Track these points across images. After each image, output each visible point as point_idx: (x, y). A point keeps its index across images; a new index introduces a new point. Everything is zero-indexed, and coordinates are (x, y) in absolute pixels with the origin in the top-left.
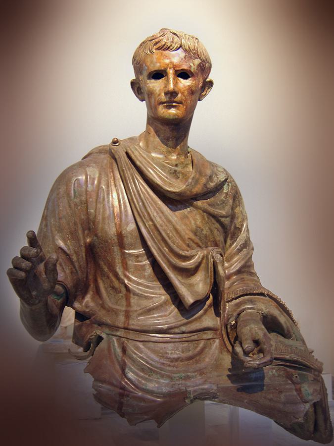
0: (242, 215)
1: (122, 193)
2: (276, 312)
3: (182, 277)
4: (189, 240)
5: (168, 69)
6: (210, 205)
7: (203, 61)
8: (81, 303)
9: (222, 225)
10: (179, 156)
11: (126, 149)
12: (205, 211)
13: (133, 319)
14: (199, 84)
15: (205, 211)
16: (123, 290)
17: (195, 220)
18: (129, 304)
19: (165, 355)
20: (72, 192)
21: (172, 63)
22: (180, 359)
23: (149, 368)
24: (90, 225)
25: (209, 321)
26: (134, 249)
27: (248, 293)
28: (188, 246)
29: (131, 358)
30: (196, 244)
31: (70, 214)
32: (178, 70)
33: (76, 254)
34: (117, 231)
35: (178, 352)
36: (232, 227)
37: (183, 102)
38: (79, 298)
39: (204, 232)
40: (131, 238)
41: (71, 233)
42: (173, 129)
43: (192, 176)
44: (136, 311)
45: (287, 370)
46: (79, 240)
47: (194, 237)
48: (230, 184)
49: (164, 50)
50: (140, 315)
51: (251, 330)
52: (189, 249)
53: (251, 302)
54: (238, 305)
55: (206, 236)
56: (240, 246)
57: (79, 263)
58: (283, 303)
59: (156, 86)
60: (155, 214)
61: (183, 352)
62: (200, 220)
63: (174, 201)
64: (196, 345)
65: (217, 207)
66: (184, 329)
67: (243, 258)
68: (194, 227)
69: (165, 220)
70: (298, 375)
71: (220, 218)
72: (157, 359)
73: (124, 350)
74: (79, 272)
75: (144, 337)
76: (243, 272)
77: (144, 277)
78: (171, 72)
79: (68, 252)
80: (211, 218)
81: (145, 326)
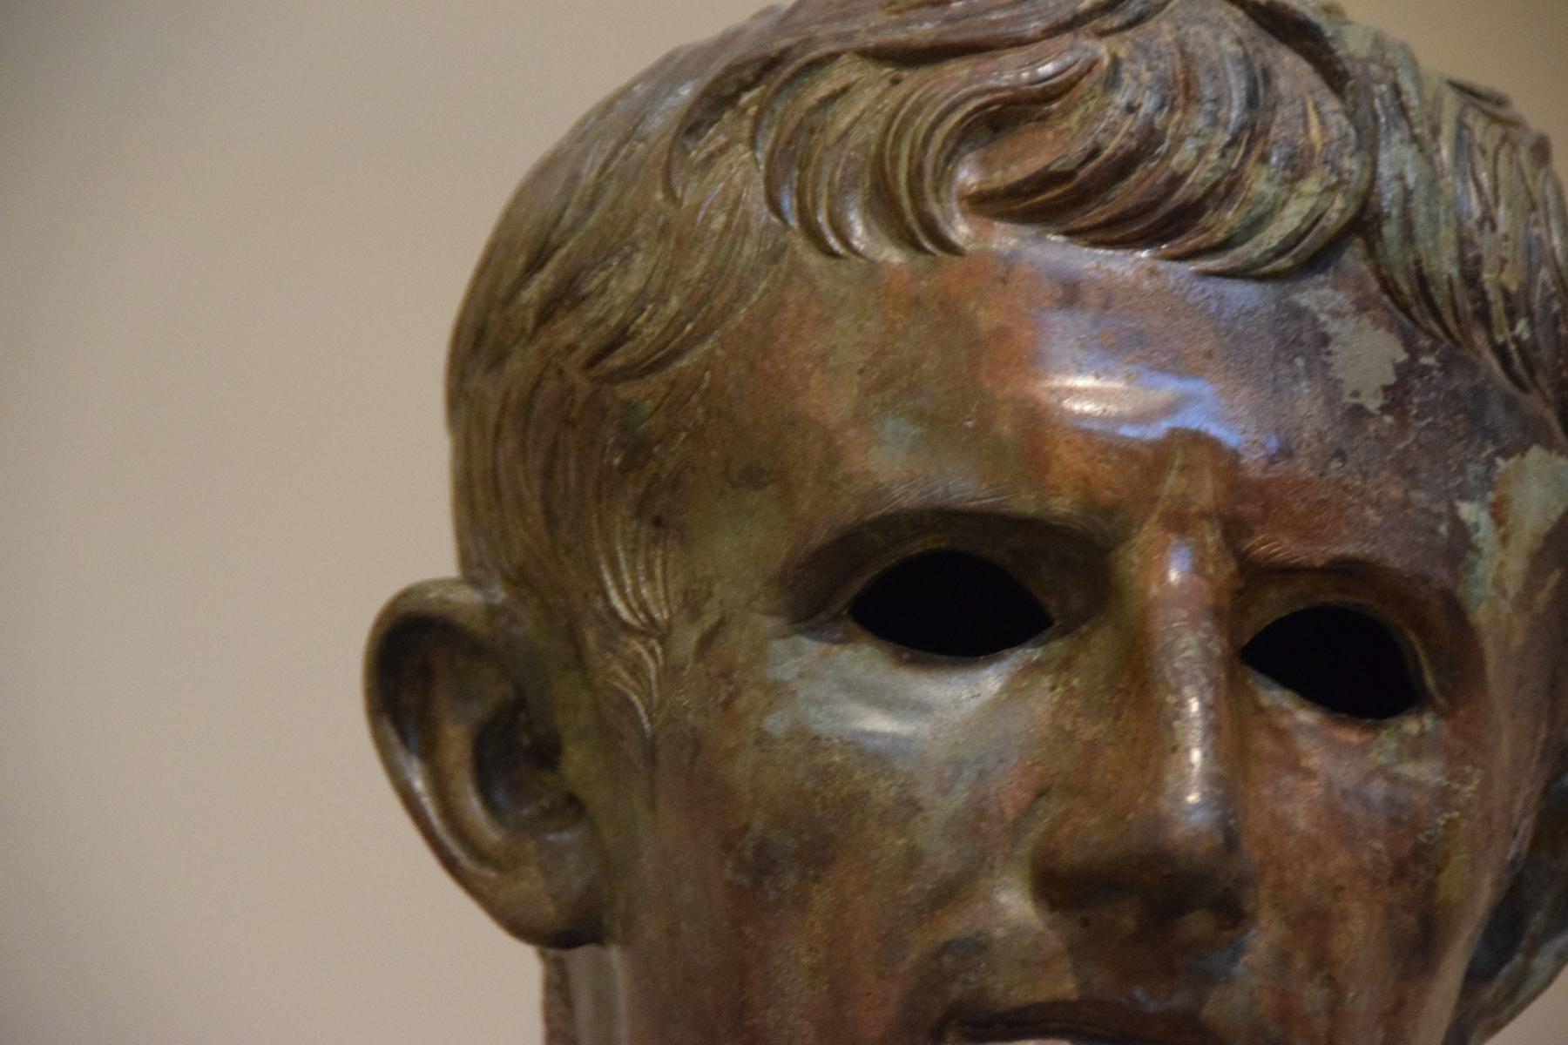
5: (1148, 533)
32: (1287, 572)
49: (1117, 233)
59: (934, 725)
78: (1173, 572)
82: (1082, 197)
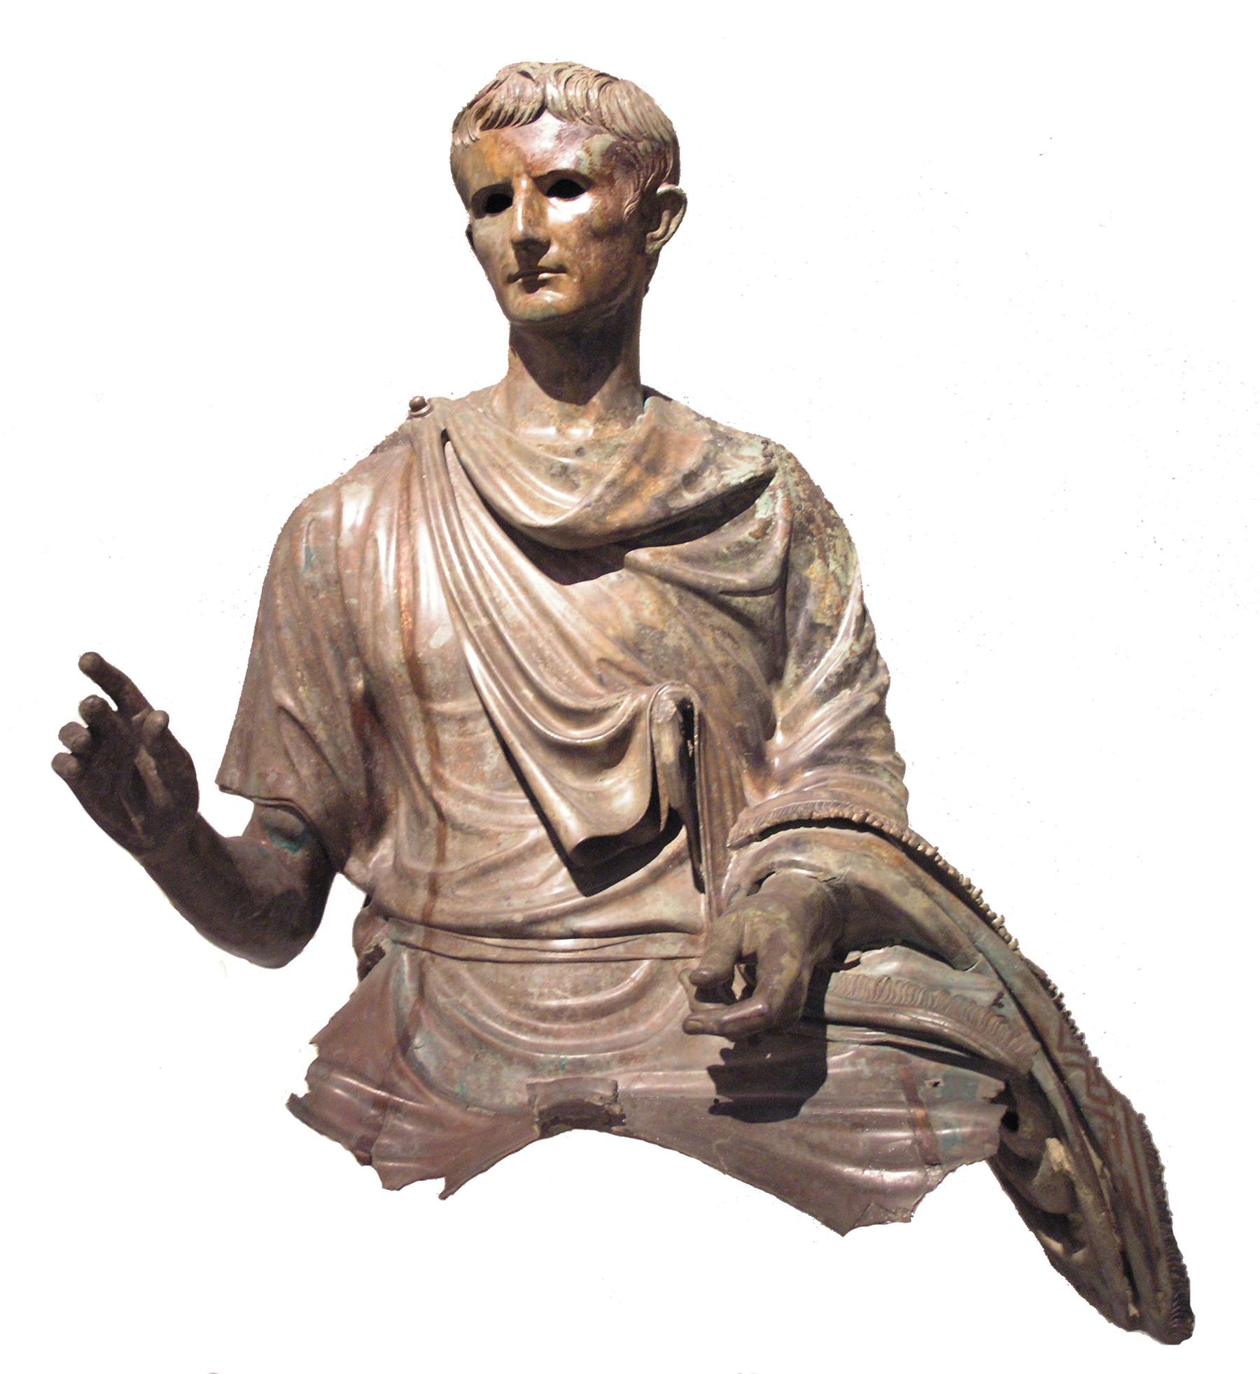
1: (444, 546)
3: (575, 771)
4: (604, 665)
6: (686, 559)
7: (626, 136)
8: (365, 862)
9: (736, 614)
10: (600, 426)
11: (445, 423)
12: (665, 578)
13: (445, 896)
14: (619, 206)
15: (665, 578)
16: (433, 815)
18: (441, 858)
19: (523, 1000)
20: (302, 555)
21: (521, 157)
22: (567, 1013)
23: (474, 1035)
24: (351, 641)
25: (666, 904)
26: (455, 697)
27: (795, 817)
28: (600, 681)
29: (434, 1006)
30: (631, 674)
31: (299, 613)
33: (326, 722)
34: (405, 650)
35: (559, 992)
36: (801, 625)
37: (568, 265)
38: (360, 846)
39: (670, 641)
40: (443, 669)
41: (309, 667)
42: (582, 346)
43: (609, 477)
44: (452, 873)
45: (906, 1061)
46: (329, 685)
47: (619, 657)
48: (780, 494)
50: (463, 882)
51: (738, 926)
52: (600, 691)
53: (796, 844)
55: (678, 653)
56: (826, 680)
57: (335, 745)
58: (929, 852)
60: (505, 595)
61: (576, 992)
62: (652, 607)
63: (567, 555)
64: (619, 974)
65: (717, 563)
67: (834, 719)
68: (632, 626)
69: (533, 612)
70: (945, 1078)
71: (727, 597)
72: (501, 1009)
74: (339, 772)
75: (470, 947)
76: (835, 761)
77: (482, 778)
78: (523, 184)
79: (301, 718)
80: (691, 597)
81: (468, 915)
82: (494, 122)
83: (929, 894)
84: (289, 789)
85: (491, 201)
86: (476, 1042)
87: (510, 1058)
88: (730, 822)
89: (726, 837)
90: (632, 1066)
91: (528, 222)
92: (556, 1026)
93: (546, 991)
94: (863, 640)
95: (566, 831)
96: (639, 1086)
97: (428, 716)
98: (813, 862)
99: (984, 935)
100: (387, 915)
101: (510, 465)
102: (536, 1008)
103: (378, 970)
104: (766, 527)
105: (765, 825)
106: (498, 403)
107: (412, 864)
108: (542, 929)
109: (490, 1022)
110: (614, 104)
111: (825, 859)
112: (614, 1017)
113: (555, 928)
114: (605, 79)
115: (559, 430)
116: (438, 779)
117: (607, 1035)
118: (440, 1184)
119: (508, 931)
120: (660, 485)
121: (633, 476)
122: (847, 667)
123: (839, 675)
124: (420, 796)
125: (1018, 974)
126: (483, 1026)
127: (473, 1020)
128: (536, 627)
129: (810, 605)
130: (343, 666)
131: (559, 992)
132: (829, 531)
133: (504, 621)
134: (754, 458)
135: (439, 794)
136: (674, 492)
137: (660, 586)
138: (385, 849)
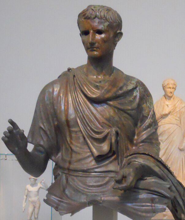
0: (149, 108)
2: (151, 164)
3: (97, 143)
5: (90, 30)
9: (128, 114)
15: (115, 107)
17: (109, 112)
18: (71, 157)
23: (77, 189)
24: (55, 115)
26: (75, 128)
28: (102, 126)
34: (66, 118)
35: (92, 182)
36: (141, 116)
47: (105, 121)
50: (76, 162)
53: (136, 158)
54: (129, 160)
55: (117, 121)
60: (85, 109)
61: (95, 183)
66: (96, 170)
73: (67, 180)
76: (145, 142)
77: (79, 143)
83: (160, 168)
84: (42, 143)
85: (85, 33)
86: (77, 191)
87: (83, 194)
88: (125, 153)
89: (124, 155)
90: (105, 195)
91: (92, 39)
92: (91, 188)
93: (90, 182)
94: (153, 119)
95: (95, 153)
96: (106, 199)
97: (70, 132)
98: (139, 161)
99: (170, 175)
100: (61, 168)
101: (87, 84)
102: (88, 185)
103: (58, 178)
104: (135, 97)
105: (131, 154)
106: (85, 70)
107: (65, 158)
108: (89, 171)
109: (80, 187)
110: (109, 16)
111: (140, 161)
112: (102, 187)
113: (92, 171)
114: (108, 11)
115: (96, 77)
116: (71, 143)
117: (100, 189)
118: (70, 214)
119: (84, 171)
120: (115, 90)
121: (110, 88)
122: (150, 124)
123: (148, 126)
124: (68, 146)
125: (176, 183)
126: (78, 188)
127: (77, 187)
128: (91, 116)
129: (143, 112)
130: (53, 120)
131: (92, 182)
132: (148, 98)
133: (85, 114)
134: (134, 83)
135: (71, 146)
136: (118, 91)
137: (114, 109)
138: (60, 155)
